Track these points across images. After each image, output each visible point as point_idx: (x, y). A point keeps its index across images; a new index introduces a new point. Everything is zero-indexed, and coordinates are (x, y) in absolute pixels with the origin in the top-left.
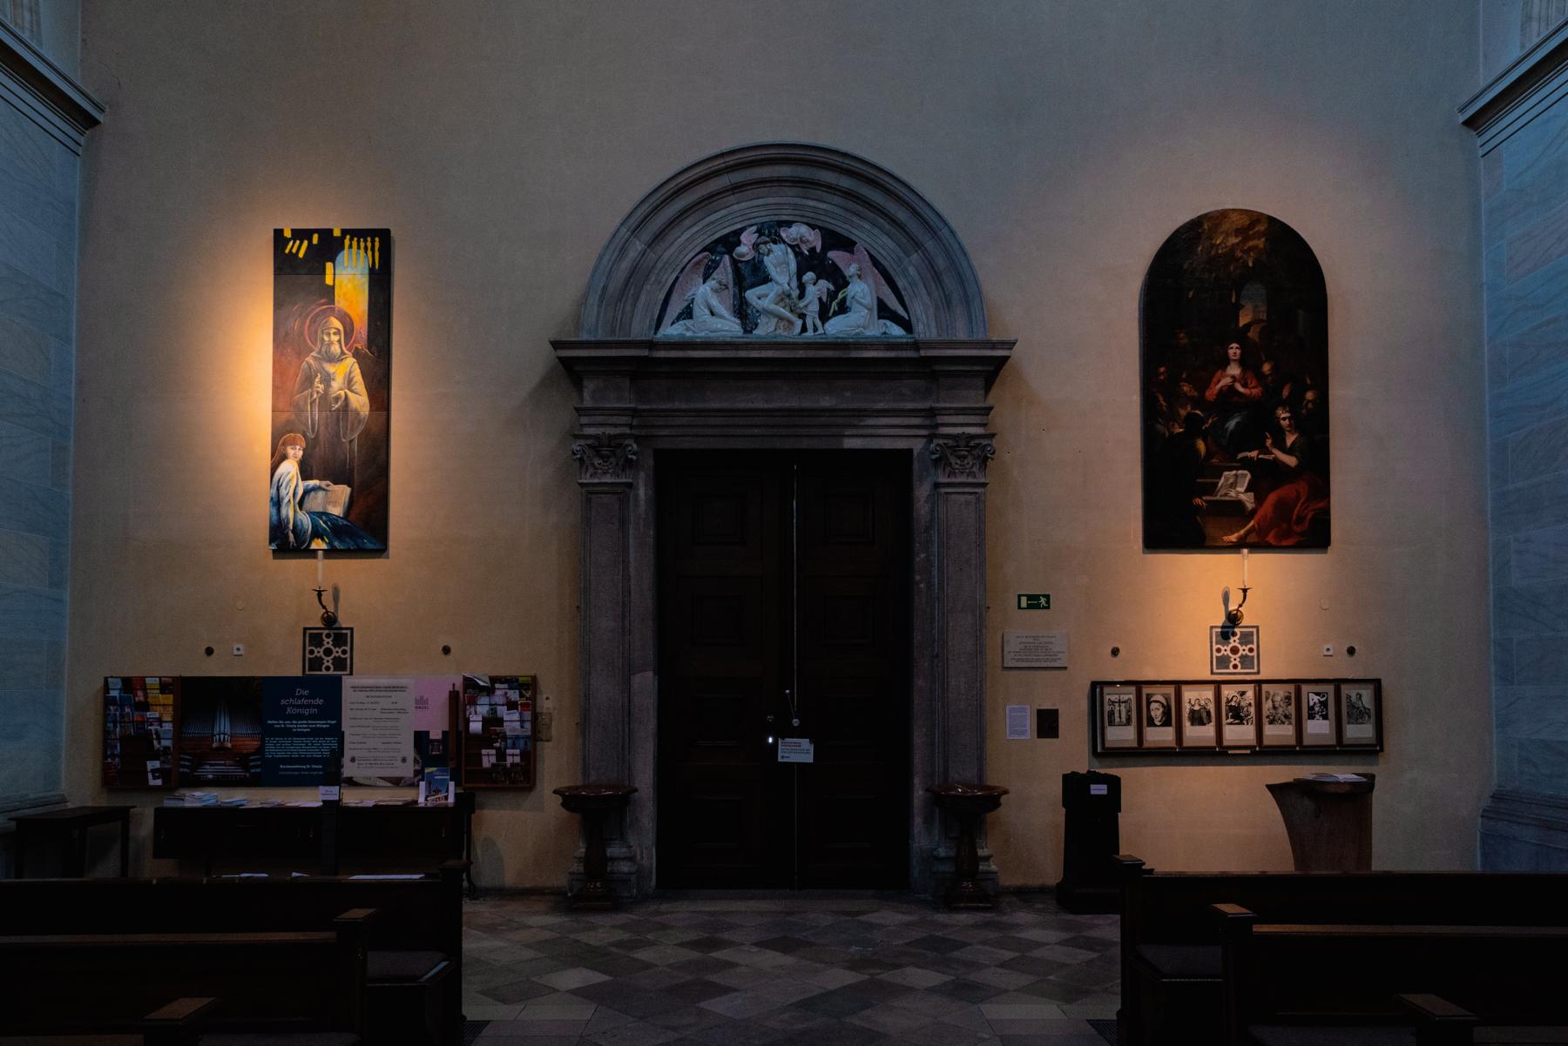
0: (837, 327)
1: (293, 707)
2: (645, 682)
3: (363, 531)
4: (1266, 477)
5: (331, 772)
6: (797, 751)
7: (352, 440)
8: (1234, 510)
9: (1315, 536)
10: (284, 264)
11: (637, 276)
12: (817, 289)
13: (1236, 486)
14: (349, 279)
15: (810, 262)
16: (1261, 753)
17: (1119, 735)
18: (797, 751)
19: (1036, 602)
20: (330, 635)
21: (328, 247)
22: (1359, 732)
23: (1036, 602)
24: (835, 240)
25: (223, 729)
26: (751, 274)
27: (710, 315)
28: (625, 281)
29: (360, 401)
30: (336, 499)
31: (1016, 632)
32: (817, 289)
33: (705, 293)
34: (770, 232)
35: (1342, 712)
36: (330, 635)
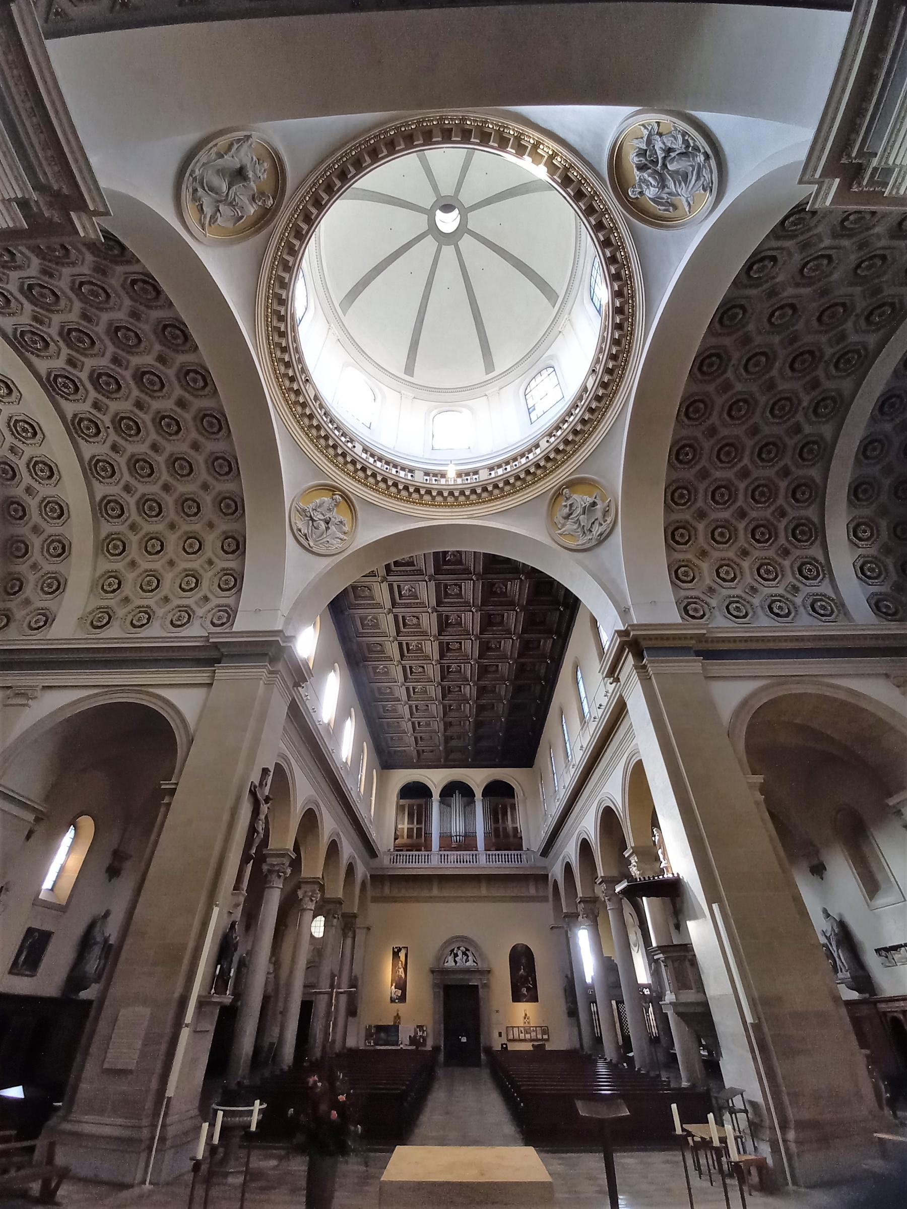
0: (468, 964)
1: (389, 1031)
2: (442, 1025)
3: (402, 999)
4: (528, 989)
5: (398, 1045)
6: (464, 1040)
7: (402, 982)
8: (524, 995)
9: (535, 999)
10: (394, 952)
11: (442, 955)
12: (465, 958)
13: (524, 991)
14: (402, 955)
15: (464, 953)
16: (531, 1040)
17: (511, 1037)
18: (464, 1040)
19: (497, 1011)
20: (398, 1017)
21: (400, 950)
22: (545, 1037)
23: (497, 1011)
24: (467, 950)
25: (382, 1035)
26: (456, 955)
27: (450, 963)
28: (440, 958)
29: (403, 976)
30: (399, 992)
31: (494, 1017)
32: (465, 958)
33: (451, 958)
34: (459, 948)
35: (544, 1033)
36: (398, 1017)
